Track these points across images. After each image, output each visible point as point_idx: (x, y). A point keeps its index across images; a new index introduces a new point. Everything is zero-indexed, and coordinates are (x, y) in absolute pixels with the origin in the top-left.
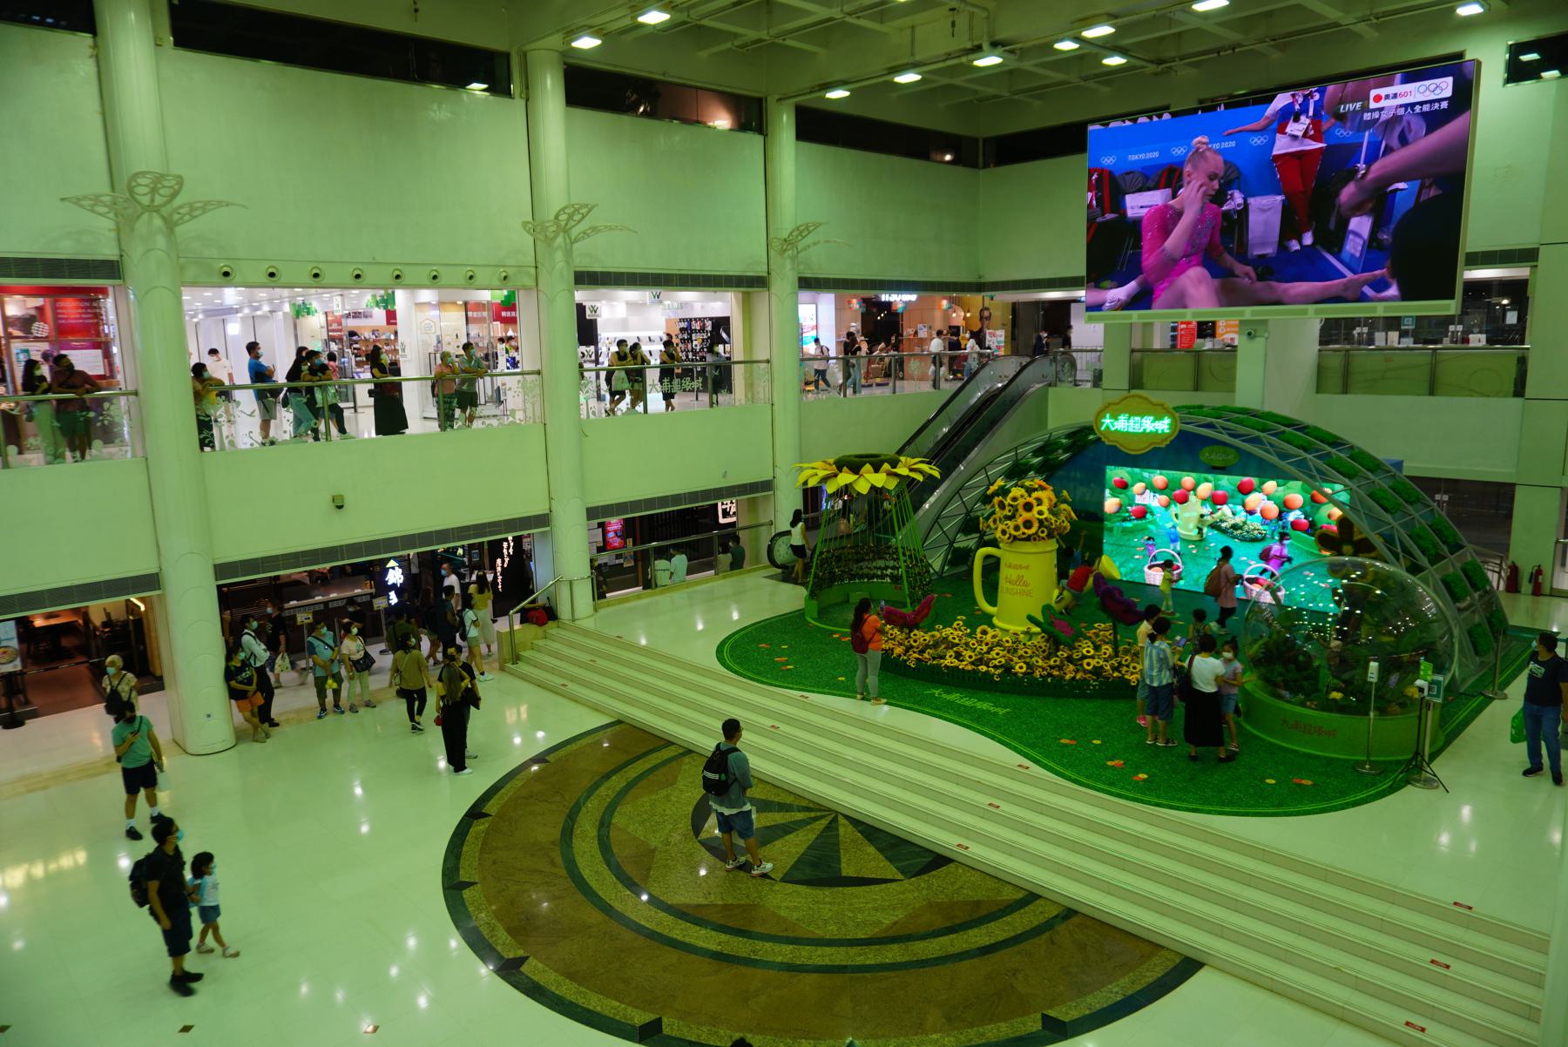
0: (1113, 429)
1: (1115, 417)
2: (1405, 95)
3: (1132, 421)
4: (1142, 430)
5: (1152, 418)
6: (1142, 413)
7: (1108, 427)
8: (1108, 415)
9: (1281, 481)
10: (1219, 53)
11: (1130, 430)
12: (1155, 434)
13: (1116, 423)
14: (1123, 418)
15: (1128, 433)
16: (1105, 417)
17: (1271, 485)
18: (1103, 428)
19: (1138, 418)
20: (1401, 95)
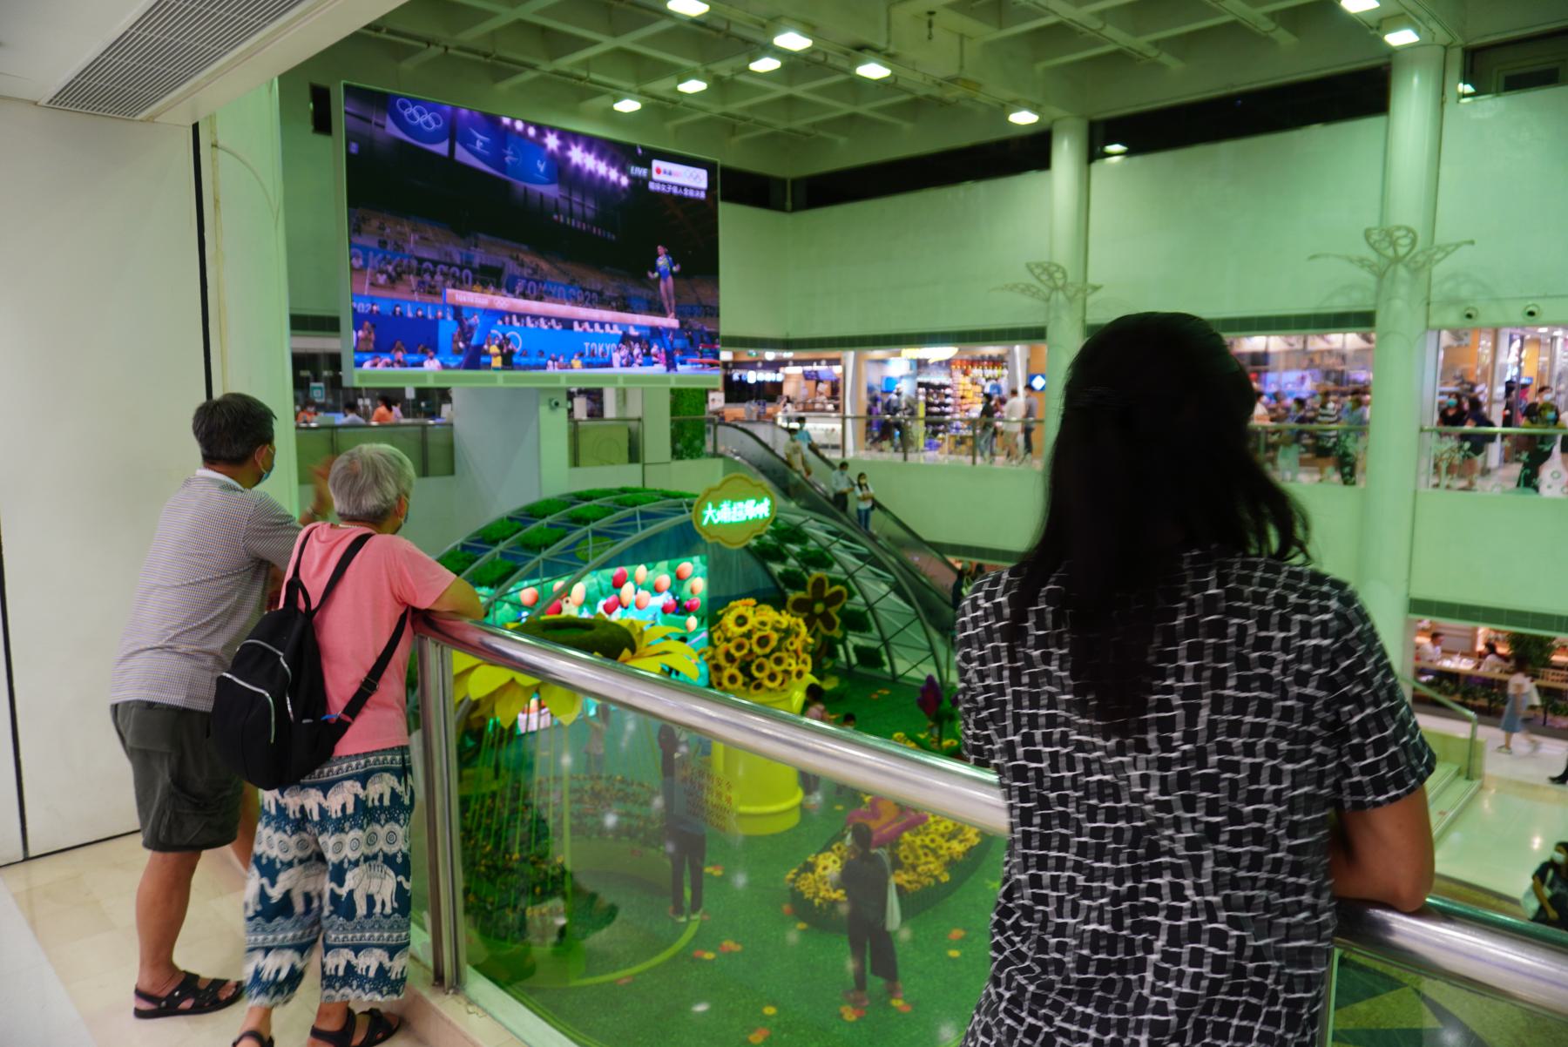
0: (716, 521)
1: (716, 506)
2: (677, 175)
3: (735, 508)
4: (744, 519)
5: (753, 501)
6: (743, 499)
7: (710, 520)
8: (710, 505)
9: (650, 565)
10: (429, 44)
11: (734, 520)
12: (756, 520)
13: (719, 513)
14: (725, 505)
15: (731, 525)
16: (706, 508)
17: (641, 571)
18: (705, 522)
19: (740, 504)
20: (677, 175)
